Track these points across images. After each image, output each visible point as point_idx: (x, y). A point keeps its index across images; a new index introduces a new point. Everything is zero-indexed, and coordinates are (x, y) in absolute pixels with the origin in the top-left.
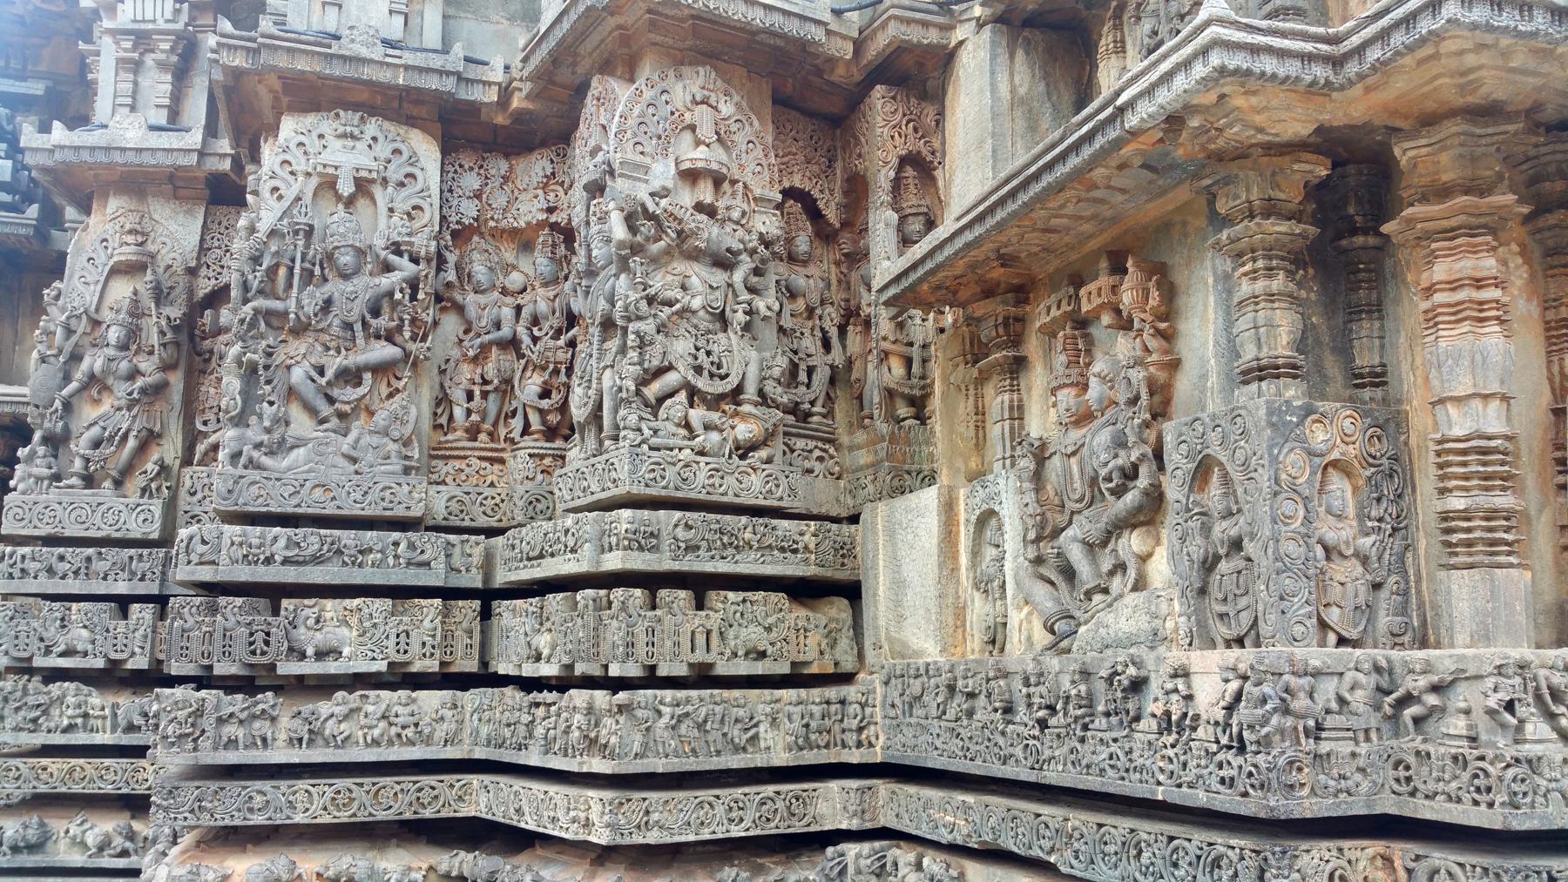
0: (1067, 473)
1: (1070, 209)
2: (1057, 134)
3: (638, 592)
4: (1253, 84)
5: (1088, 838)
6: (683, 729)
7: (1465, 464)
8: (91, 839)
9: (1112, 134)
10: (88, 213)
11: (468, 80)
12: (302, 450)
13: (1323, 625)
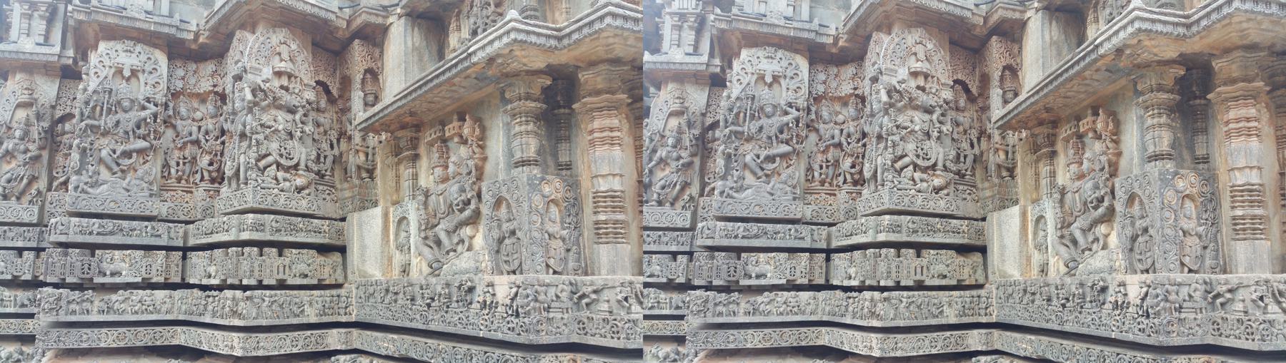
0: (1074, 200)
1: (1075, 88)
2: (1070, 57)
3: (892, 250)
4: (1153, 36)
5: (1083, 354)
6: (911, 308)
7: (1242, 196)
8: (661, 354)
9: (1093, 56)
10: (660, 90)
11: (820, 34)
12: (750, 190)
13: (1183, 264)
